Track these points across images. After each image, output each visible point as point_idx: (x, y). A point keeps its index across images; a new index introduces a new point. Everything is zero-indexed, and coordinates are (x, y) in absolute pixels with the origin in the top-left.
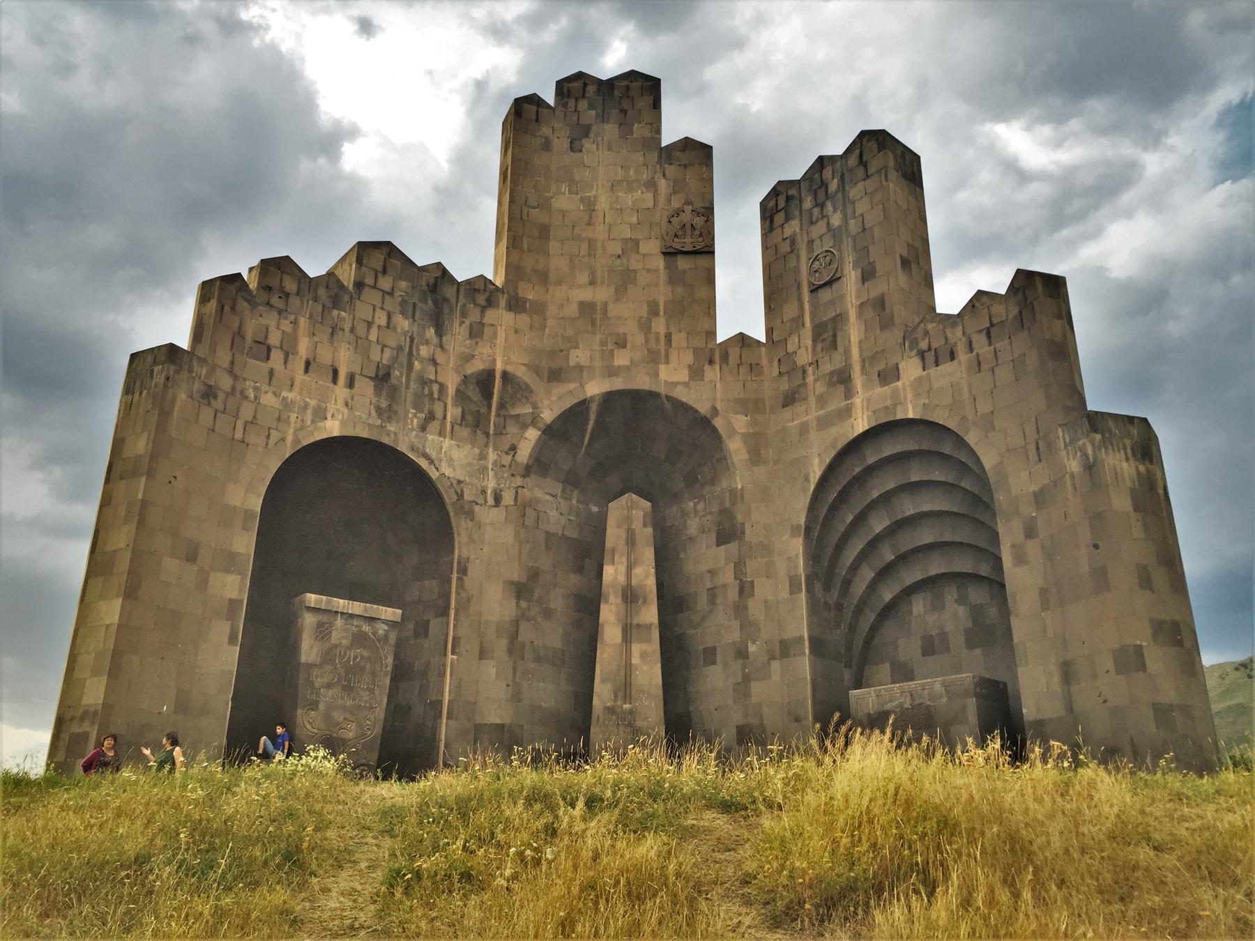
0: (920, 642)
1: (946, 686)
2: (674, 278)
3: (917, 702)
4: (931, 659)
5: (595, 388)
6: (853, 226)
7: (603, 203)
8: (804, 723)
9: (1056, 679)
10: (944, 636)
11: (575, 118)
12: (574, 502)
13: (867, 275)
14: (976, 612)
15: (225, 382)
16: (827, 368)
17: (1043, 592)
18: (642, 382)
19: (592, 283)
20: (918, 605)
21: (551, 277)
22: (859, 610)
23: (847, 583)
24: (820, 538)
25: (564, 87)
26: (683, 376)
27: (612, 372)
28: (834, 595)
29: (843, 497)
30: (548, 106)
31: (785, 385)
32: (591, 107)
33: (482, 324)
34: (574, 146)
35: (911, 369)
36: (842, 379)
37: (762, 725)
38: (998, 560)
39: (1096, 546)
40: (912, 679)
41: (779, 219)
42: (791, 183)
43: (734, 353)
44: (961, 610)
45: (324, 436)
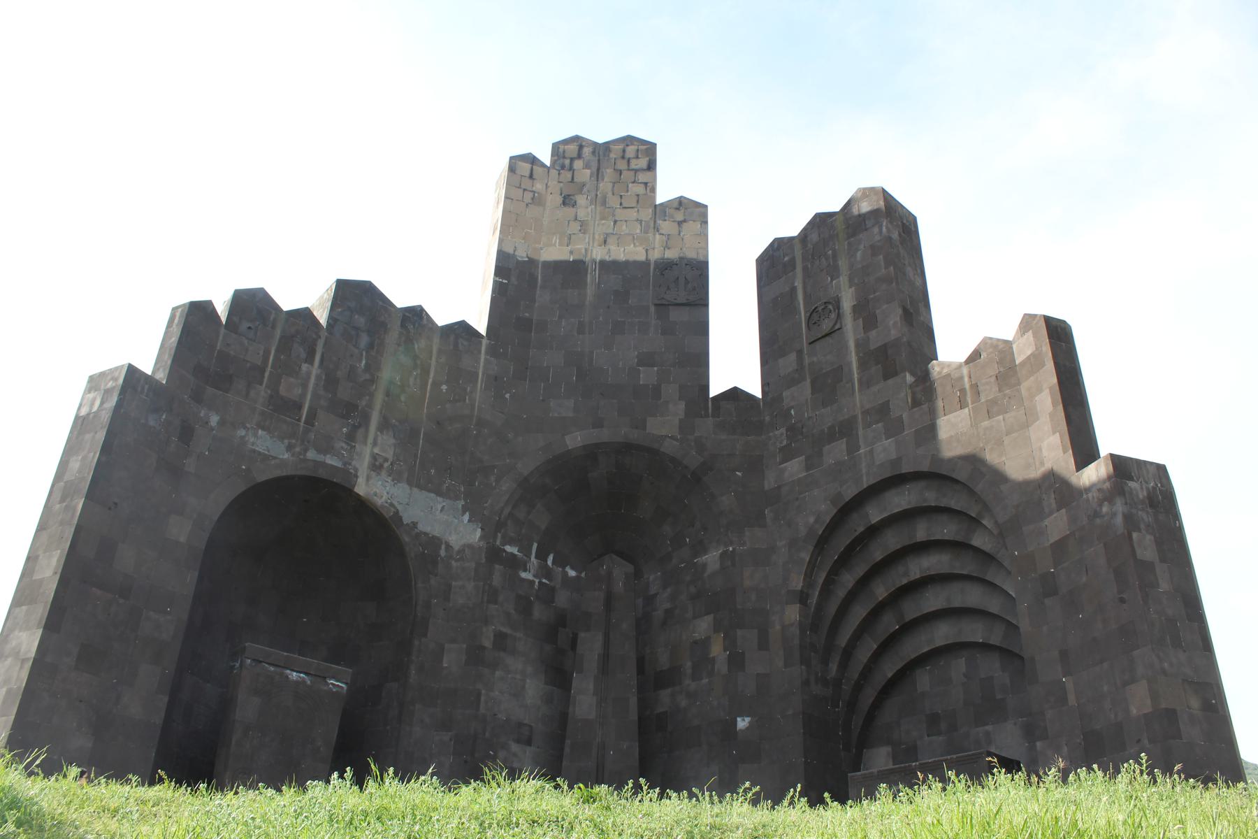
11: (569, 175)
12: (550, 562)
20: (924, 680)
22: (858, 687)
23: (848, 653)
24: (820, 607)
25: (557, 149)
27: (598, 424)
28: (834, 667)
29: (845, 560)
30: (543, 165)
32: (587, 166)
38: (1012, 628)
39: (1122, 601)
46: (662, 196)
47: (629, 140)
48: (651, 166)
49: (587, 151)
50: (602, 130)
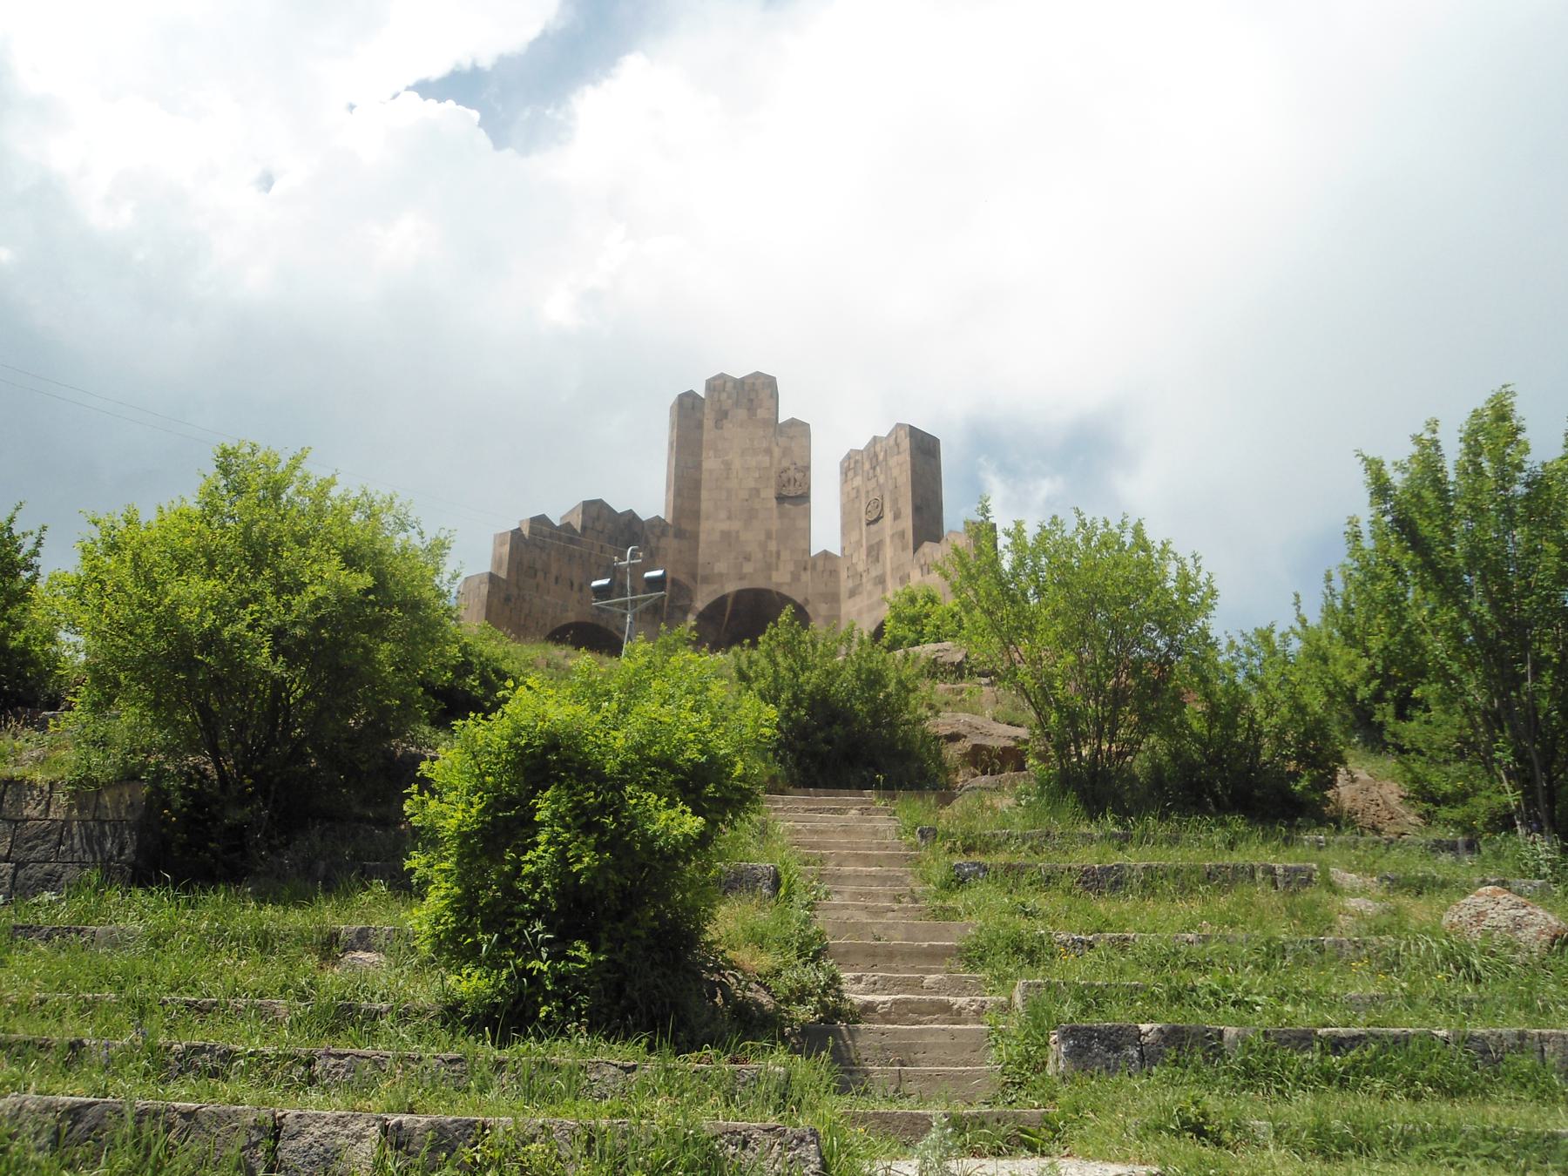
2: (782, 516)
5: (731, 588)
6: (890, 485)
7: (737, 464)
13: (897, 517)
15: (515, 591)
16: (874, 573)
18: (760, 583)
19: (729, 518)
21: (703, 514)
26: (787, 578)
31: (850, 584)
33: (657, 548)
34: (718, 424)
35: (916, 576)
36: (881, 581)
41: (851, 474)
42: (858, 452)
43: (820, 563)
45: (564, 622)
46: (783, 417)
47: (757, 375)
48: (774, 396)
49: (729, 385)
50: (739, 370)
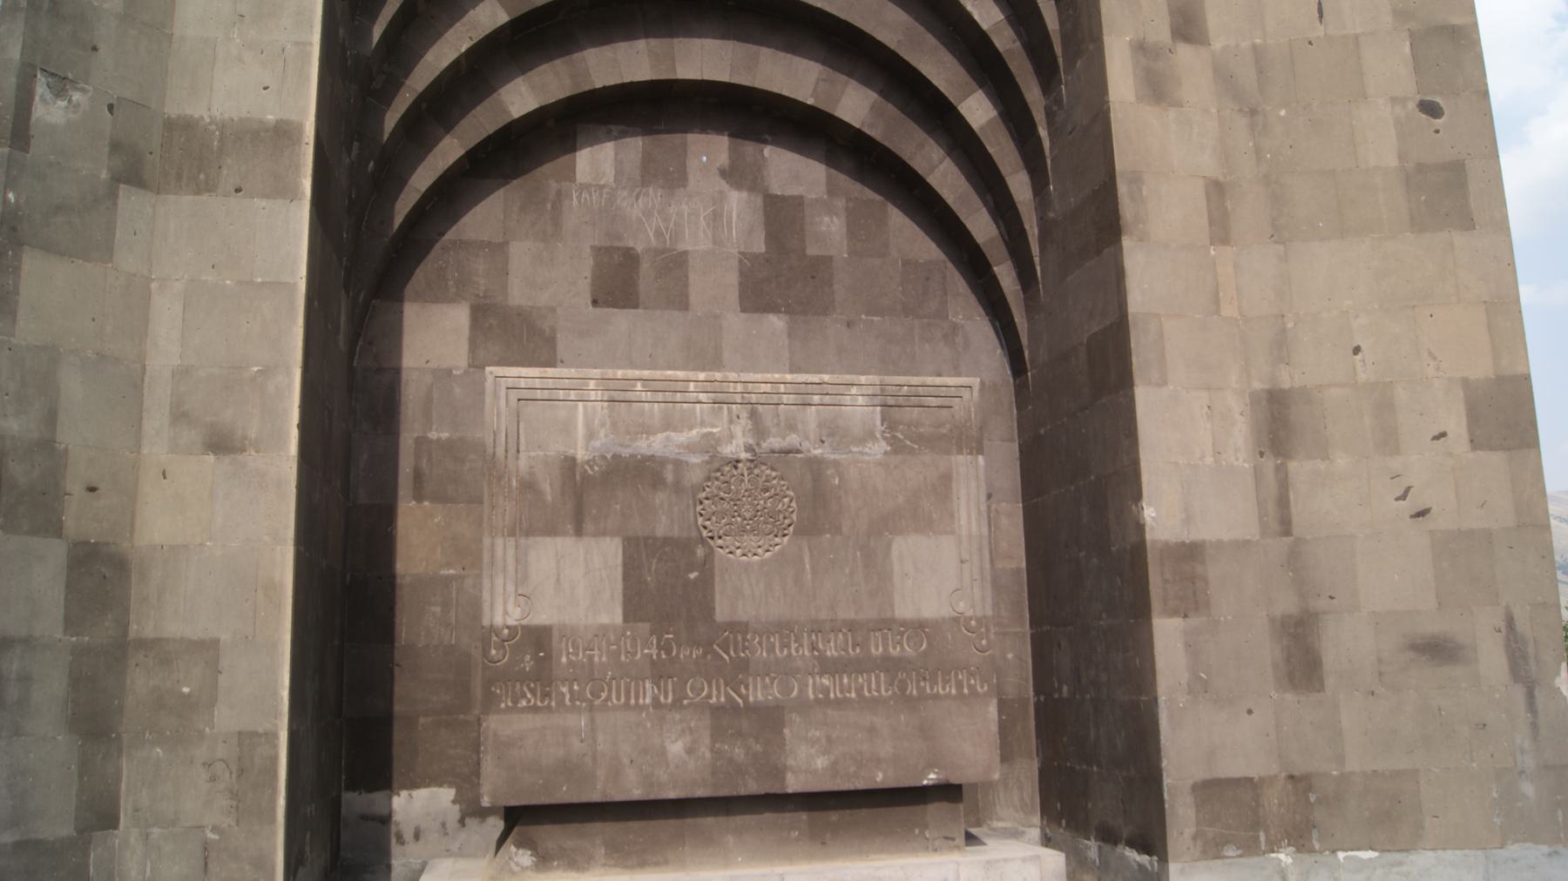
0: (587, 265)
1: (889, 406)
3: (774, 442)
4: (621, 320)
8: (252, 459)
9: (1240, 434)
10: (674, 264)
14: (782, 216)
17: (1217, 190)
20: (599, 162)
37: (47, 446)
40: (551, 363)
44: (737, 202)
